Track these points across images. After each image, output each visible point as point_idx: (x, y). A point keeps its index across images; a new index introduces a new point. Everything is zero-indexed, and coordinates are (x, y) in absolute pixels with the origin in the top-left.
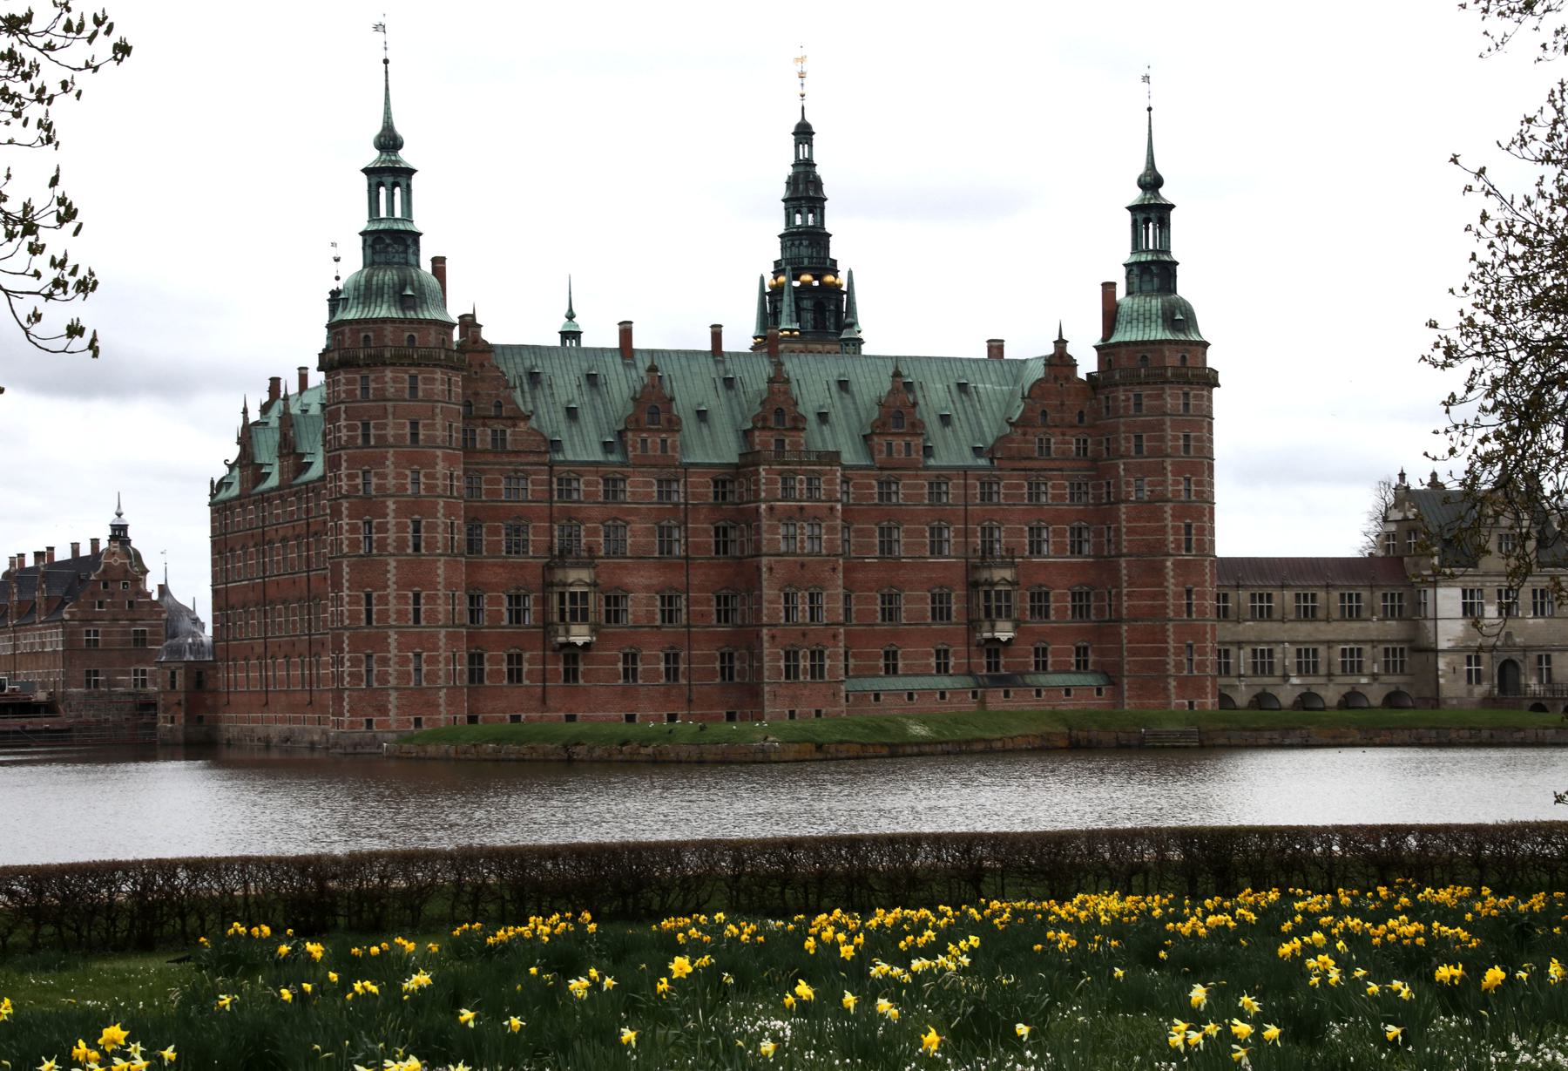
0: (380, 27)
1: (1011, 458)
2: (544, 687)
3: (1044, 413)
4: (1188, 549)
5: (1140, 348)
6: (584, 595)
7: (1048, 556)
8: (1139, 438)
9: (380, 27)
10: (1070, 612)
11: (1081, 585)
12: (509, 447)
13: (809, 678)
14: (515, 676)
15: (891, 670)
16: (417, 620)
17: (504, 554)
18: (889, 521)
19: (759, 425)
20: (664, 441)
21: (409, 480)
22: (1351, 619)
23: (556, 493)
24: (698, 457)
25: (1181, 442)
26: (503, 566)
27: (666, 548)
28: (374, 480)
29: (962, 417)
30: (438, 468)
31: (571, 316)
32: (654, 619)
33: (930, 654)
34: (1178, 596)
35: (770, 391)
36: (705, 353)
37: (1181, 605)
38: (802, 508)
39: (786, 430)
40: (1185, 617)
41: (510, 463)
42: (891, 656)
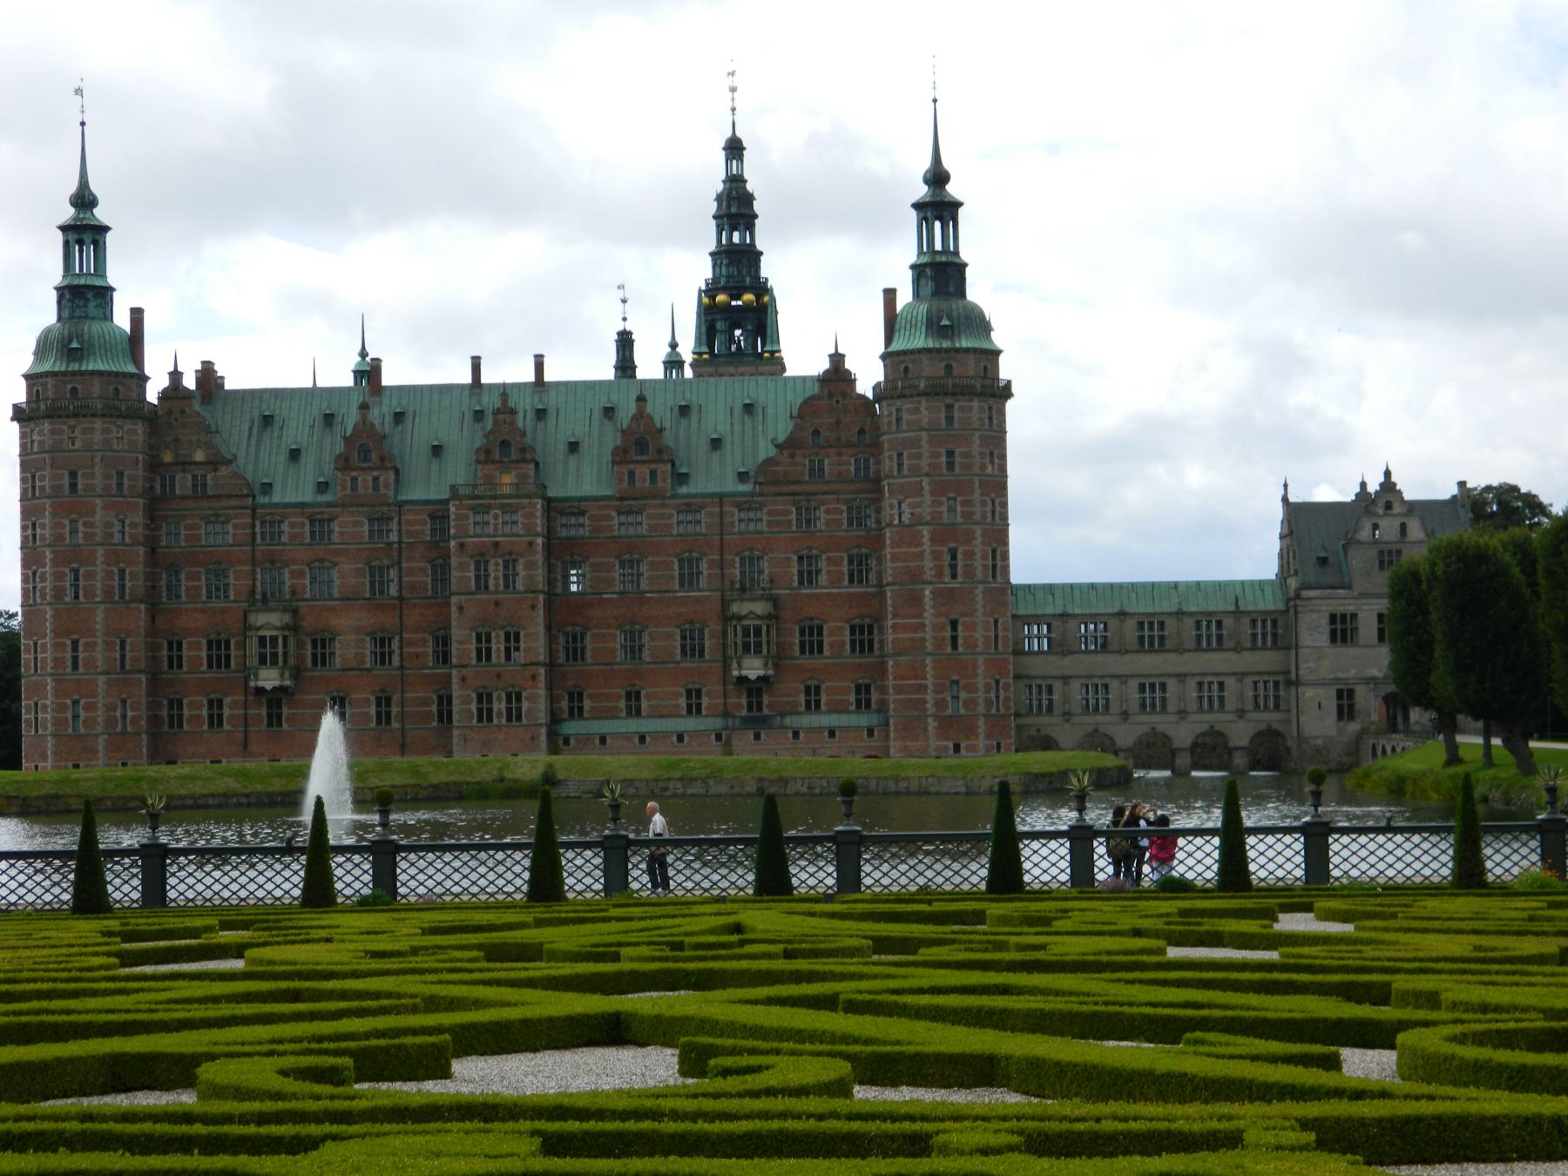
1: (776, 482)
2: (246, 733)
3: (816, 433)
4: (954, 576)
5: (902, 358)
6: (274, 639)
7: (822, 587)
8: (900, 455)
9: (79, 92)
10: (848, 647)
11: (861, 617)
12: (210, 492)
13: (504, 721)
14: (216, 721)
15: (635, 712)
16: (75, 666)
17: (204, 599)
18: (631, 553)
19: (482, 458)
20: (375, 479)
21: (67, 529)
22: (1152, 650)
23: (258, 536)
24: (416, 492)
25: (944, 459)
26: (202, 611)
27: (378, 586)
28: (38, 531)
29: (736, 440)
30: (97, 516)
32: (363, 662)
33: (678, 695)
34: (938, 627)
35: (496, 423)
36: (461, 387)
37: (944, 638)
38: (496, 544)
39: (512, 462)
40: (949, 649)
41: (209, 509)
42: (633, 697)
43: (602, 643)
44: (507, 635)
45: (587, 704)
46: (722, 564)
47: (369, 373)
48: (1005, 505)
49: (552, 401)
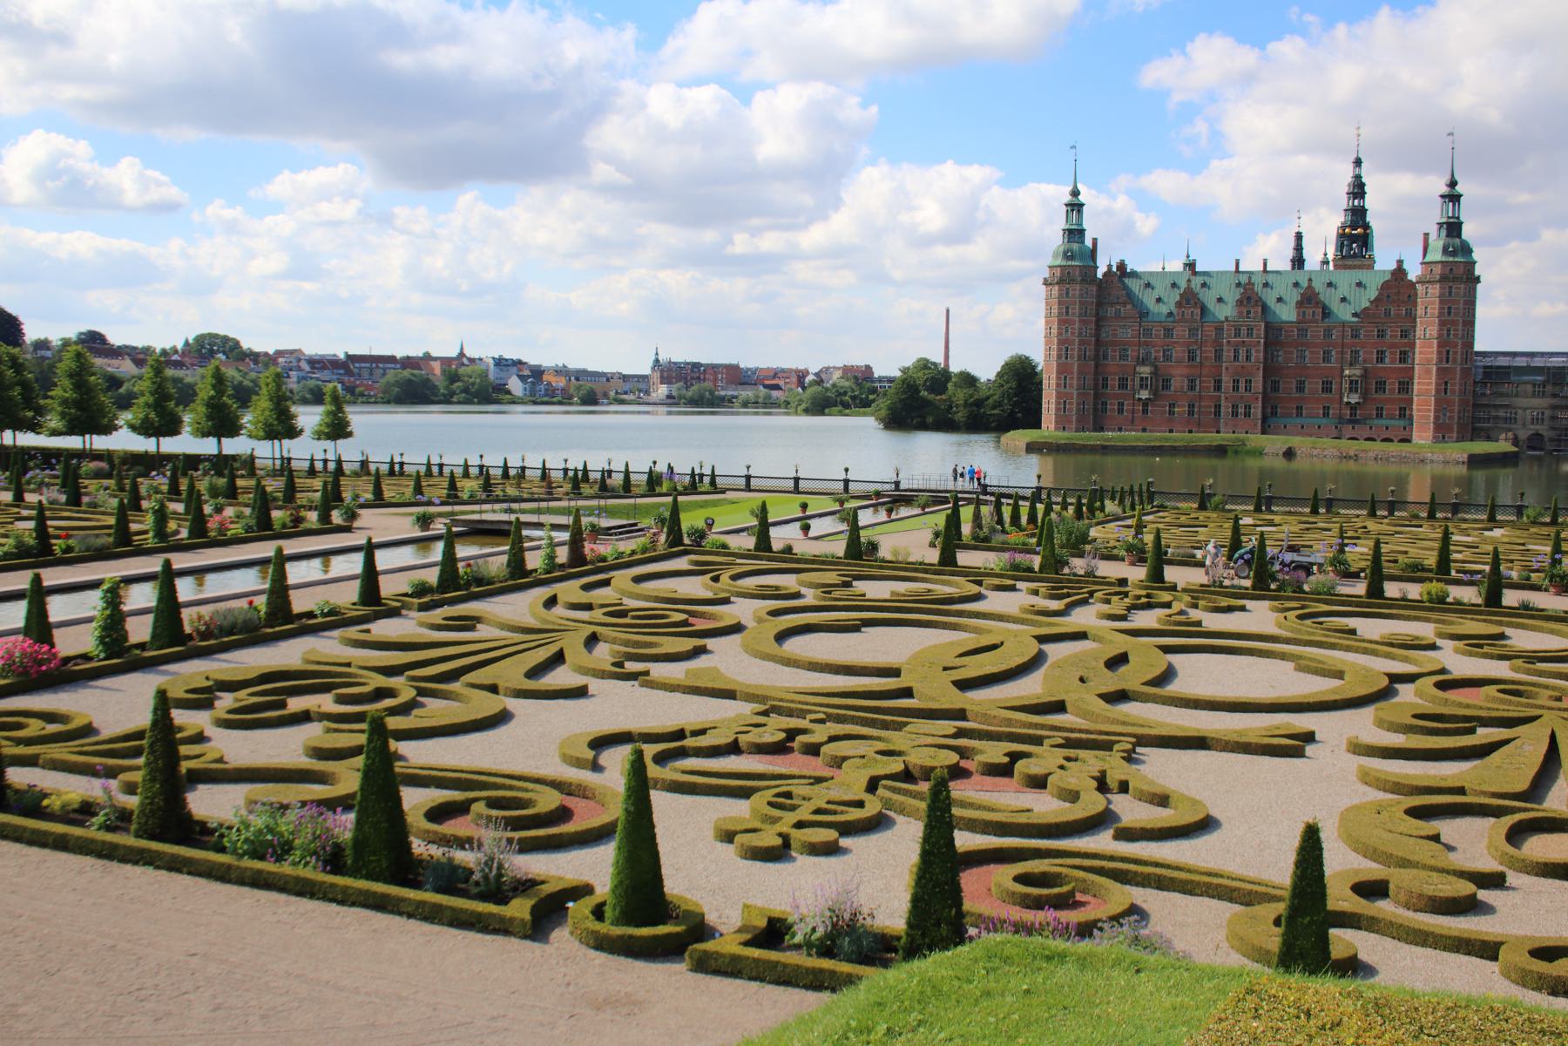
0: (1074, 147)
3: (1388, 296)
4: (1447, 362)
6: (1147, 378)
9: (1074, 147)
15: (1299, 414)
16: (1065, 387)
31: (1188, 256)
33: (1319, 408)
36: (1231, 272)
42: (1299, 408)
43: (1288, 385)
44: (1246, 381)
45: (1279, 410)
46: (1342, 353)
47: (1191, 266)
48: (1473, 331)
49: (1270, 279)
